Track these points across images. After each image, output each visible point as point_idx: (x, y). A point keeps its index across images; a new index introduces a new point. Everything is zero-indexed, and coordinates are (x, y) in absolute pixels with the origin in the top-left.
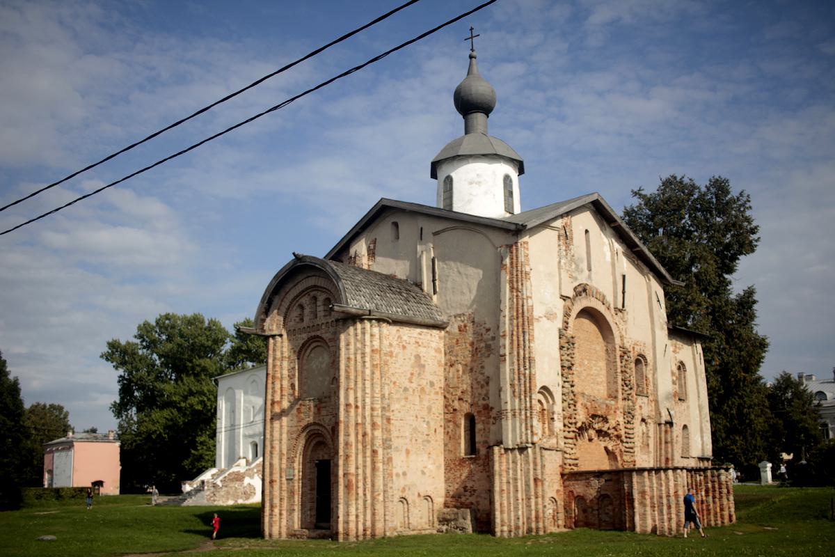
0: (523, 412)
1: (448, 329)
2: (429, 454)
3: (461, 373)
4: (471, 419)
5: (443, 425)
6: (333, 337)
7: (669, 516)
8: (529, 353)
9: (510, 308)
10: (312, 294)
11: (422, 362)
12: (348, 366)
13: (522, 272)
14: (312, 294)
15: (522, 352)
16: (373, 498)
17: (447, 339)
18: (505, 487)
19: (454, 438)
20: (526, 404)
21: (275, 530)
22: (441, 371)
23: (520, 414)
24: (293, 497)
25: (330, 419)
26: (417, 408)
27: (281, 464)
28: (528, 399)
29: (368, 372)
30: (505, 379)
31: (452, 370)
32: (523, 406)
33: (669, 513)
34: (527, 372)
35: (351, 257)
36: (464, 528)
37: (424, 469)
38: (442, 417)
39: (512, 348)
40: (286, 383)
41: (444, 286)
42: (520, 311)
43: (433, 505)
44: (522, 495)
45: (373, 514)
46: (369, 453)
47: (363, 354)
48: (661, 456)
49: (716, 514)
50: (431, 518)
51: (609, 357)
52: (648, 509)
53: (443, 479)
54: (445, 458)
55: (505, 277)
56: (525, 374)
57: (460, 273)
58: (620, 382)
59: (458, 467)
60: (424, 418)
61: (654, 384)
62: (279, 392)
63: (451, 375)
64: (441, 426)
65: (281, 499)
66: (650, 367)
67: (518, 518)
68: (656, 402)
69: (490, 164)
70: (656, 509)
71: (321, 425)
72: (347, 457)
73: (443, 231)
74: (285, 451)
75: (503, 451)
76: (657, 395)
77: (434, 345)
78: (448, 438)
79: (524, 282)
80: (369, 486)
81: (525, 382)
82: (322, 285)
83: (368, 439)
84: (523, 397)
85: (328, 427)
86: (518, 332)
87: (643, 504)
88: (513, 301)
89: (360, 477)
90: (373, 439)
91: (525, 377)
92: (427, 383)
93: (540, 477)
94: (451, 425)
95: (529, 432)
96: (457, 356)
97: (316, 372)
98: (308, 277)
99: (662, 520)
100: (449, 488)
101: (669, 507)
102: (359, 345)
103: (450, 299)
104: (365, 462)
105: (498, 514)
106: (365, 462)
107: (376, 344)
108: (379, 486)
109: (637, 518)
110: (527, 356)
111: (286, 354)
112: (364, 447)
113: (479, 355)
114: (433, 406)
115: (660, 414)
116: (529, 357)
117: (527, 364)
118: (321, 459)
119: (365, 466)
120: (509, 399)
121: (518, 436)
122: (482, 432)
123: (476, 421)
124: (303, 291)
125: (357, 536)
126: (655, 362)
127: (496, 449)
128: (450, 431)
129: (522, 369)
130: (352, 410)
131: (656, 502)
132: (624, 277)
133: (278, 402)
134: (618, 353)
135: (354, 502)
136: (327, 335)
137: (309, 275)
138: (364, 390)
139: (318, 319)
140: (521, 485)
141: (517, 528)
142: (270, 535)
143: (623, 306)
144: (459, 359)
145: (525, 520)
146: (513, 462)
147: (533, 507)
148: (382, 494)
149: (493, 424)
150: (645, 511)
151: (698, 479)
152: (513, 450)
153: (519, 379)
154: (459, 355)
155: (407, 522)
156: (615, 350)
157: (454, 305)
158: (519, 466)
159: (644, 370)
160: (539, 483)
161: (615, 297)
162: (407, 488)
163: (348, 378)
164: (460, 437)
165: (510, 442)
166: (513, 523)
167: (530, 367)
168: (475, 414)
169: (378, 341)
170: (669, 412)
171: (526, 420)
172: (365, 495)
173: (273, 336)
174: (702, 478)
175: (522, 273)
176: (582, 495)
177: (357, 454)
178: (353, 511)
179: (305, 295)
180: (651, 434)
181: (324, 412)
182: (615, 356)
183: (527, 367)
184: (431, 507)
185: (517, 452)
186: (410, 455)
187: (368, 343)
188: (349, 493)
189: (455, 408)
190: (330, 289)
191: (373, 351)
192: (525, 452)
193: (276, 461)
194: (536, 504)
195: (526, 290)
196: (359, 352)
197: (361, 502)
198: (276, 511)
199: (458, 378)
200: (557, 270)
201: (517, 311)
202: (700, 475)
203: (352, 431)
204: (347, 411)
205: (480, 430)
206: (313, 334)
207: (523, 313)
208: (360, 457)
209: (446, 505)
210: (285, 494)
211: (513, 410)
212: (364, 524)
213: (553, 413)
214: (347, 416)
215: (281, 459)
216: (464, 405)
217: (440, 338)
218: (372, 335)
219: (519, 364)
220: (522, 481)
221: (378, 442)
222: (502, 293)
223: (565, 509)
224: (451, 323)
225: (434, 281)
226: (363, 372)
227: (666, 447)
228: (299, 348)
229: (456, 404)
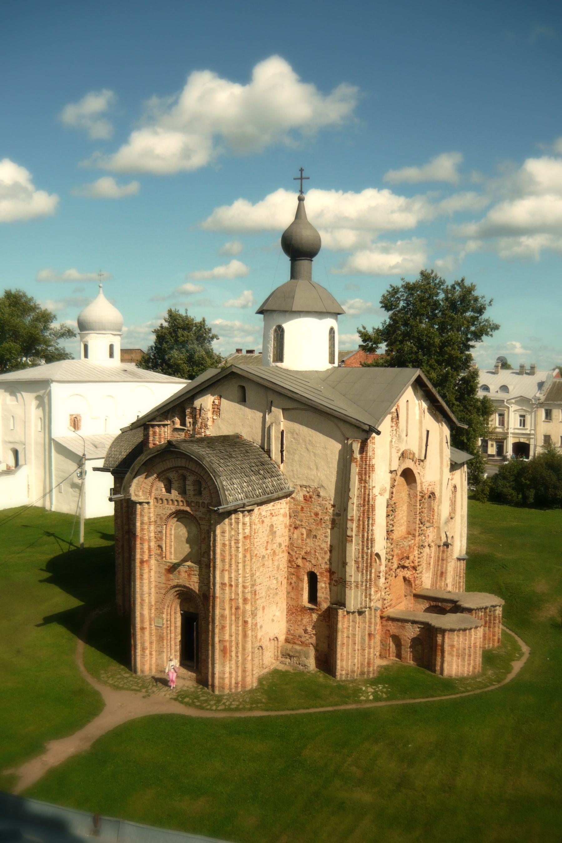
0: (364, 584)
1: (293, 496)
2: (277, 603)
3: (305, 536)
4: (313, 579)
5: (286, 576)
6: (204, 516)
7: (469, 662)
8: (372, 535)
9: (358, 497)
11: (275, 529)
12: (223, 551)
13: (369, 465)
15: (366, 534)
16: (244, 660)
17: (292, 504)
18: (345, 641)
19: (297, 589)
20: (367, 578)
21: (147, 667)
22: (286, 532)
23: (362, 585)
24: (163, 642)
26: (270, 569)
27: (150, 613)
28: (368, 573)
29: (240, 555)
30: (351, 556)
31: (296, 532)
32: (365, 578)
33: (469, 660)
34: (369, 551)
35: (195, 408)
36: (306, 665)
37: (274, 618)
38: (286, 570)
39: (358, 531)
40: (153, 544)
41: (291, 456)
42: (367, 499)
43: (278, 643)
44: (358, 646)
45: (244, 671)
46: (240, 623)
47: (237, 541)
48: (438, 571)
49: (490, 639)
50: (276, 653)
51: (411, 500)
52: (455, 658)
53: (285, 620)
54: (288, 603)
55: (355, 469)
56: (367, 553)
57: (308, 450)
58: (418, 522)
59: (300, 613)
60: (274, 576)
61: (438, 514)
62: (147, 551)
63: (295, 536)
64: (285, 578)
65: (151, 643)
66: (437, 500)
67: (355, 665)
68: (439, 528)
69: (320, 319)
70: (460, 657)
72: (223, 627)
73: (293, 409)
74: (153, 603)
75: (345, 613)
76: (440, 522)
77: (282, 511)
78: (291, 588)
79: (371, 474)
80: (240, 649)
81: (367, 559)
83: (240, 611)
84: (364, 571)
86: (364, 518)
87: (451, 654)
88: (361, 491)
89: (234, 643)
90: (244, 612)
91: (367, 555)
92: (277, 546)
93: (373, 633)
94: (294, 579)
95: (368, 599)
96: (301, 521)
99: (463, 666)
100: (290, 627)
101: (470, 656)
102: (233, 533)
103: (297, 471)
104: (237, 630)
105: (339, 662)
106: (237, 630)
107: (247, 531)
108: (249, 649)
109: (445, 665)
110: (370, 538)
111: (152, 519)
112: (237, 618)
113: (324, 525)
114: (280, 563)
115: (441, 538)
116: (371, 539)
117: (370, 544)
118: (186, 610)
119: (237, 634)
120: (353, 573)
121: (359, 603)
122: (323, 590)
123: (318, 580)
124: (171, 468)
125: (230, 689)
126: (441, 496)
127: (340, 612)
128: (293, 582)
129: (365, 548)
130: (227, 588)
131: (460, 652)
132: (428, 432)
133: (147, 561)
134: (419, 498)
135: (228, 662)
136: (197, 513)
138: (237, 571)
140: (358, 639)
141: (353, 672)
142: (142, 671)
143: (425, 457)
144: (303, 524)
145: (359, 665)
146: (353, 621)
147: (366, 656)
148: (250, 654)
149: (334, 585)
150: (452, 659)
151: (480, 615)
152: (353, 613)
153: (363, 557)
154: (304, 521)
155: (261, 664)
156: (416, 496)
157: (301, 476)
158: (357, 625)
159: (432, 504)
160: (373, 637)
161: (420, 450)
162: (262, 638)
163: (223, 561)
164: (302, 589)
165: (352, 607)
166: (349, 669)
167: (372, 547)
168: (318, 574)
169: (249, 528)
170: (446, 535)
171: (366, 590)
172: (237, 657)
173: (141, 503)
174: (483, 614)
175: (369, 467)
176: (397, 634)
177: (231, 625)
178: (227, 669)
179: (173, 471)
180: (433, 555)
182: (416, 501)
183: (369, 547)
184: (276, 644)
185: (357, 614)
186: (265, 610)
187: (241, 531)
188: (224, 657)
189: (298, 564)
191: (245, 537)
192: (364, 614)
193: (146, 612)
194: (369, 653)
195: (372, 481)
196: (233, 538)
197: (233, 662)
198: (147, 652)
199: (303, 540)
200: (388, 449)
201: (364, 500)
202: (481, 612)
203: (227, 606)
204: (223, 590)
205: (322, 588)
207: (369, 501)
208: (233, 627)
209: (287, 641)
210: (154, 638)
211: (357, 582)
212: (236, 679)
213: (380, 572)
214: (224, 593)
215: (150, 610)
216: (307, 564)
217: (286, 503)
218: (244, 524)
219: (363, 545)
220: (359, 635)
221: (249, 613)
222: (351, 483)
223: (381, 642)
224: (296, 491)
225: (282, 451)
226: (236, 556)
227: (443, 564)
229: (300, 562)
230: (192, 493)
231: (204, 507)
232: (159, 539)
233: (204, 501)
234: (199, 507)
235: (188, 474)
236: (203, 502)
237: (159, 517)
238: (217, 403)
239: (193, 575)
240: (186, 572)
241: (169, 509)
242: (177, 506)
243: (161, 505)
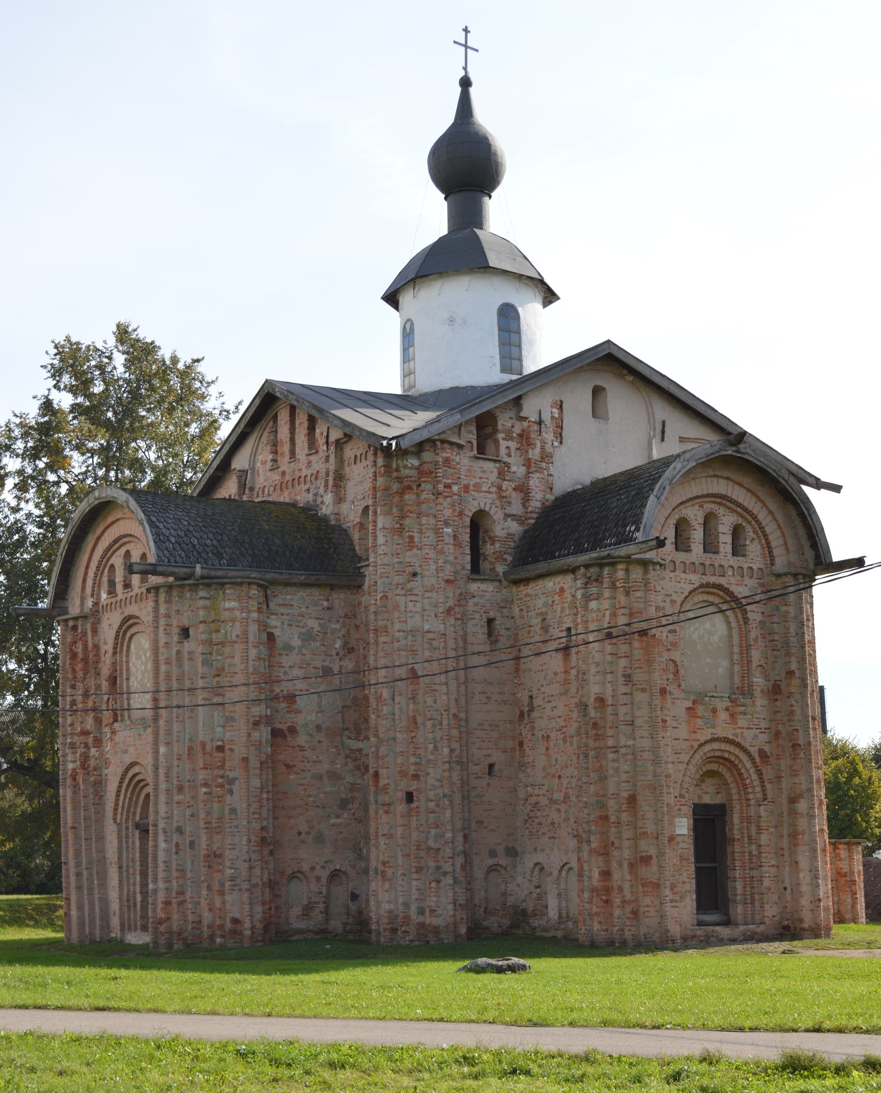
10: (708, 507)
14: (708, 507)
25: (756, 736)
71: (738, 745)
82: (746, 505)
85: (752, 750)
97: (699, 647)
98: (715, 476)
118: (696, 801)
136: (741, 589)
137: (719, 473)
139: (721, 555)
179: (693, 505)
181: (742, 722)
190: (755, 512)
206: (712, 580)
228: (683, 596)
230: (729, 548)
231: (751, 578)
232: (669, 647)
233: (751, 565)
234: (743, 577)
235: (721, 511)
236: (751, 568)
237: (668, 599)
238: (557, 416)
239: (740, 713)
240: (727, 709)
241: (688, 581)
242: (704, 577)
243: (672, 574)
